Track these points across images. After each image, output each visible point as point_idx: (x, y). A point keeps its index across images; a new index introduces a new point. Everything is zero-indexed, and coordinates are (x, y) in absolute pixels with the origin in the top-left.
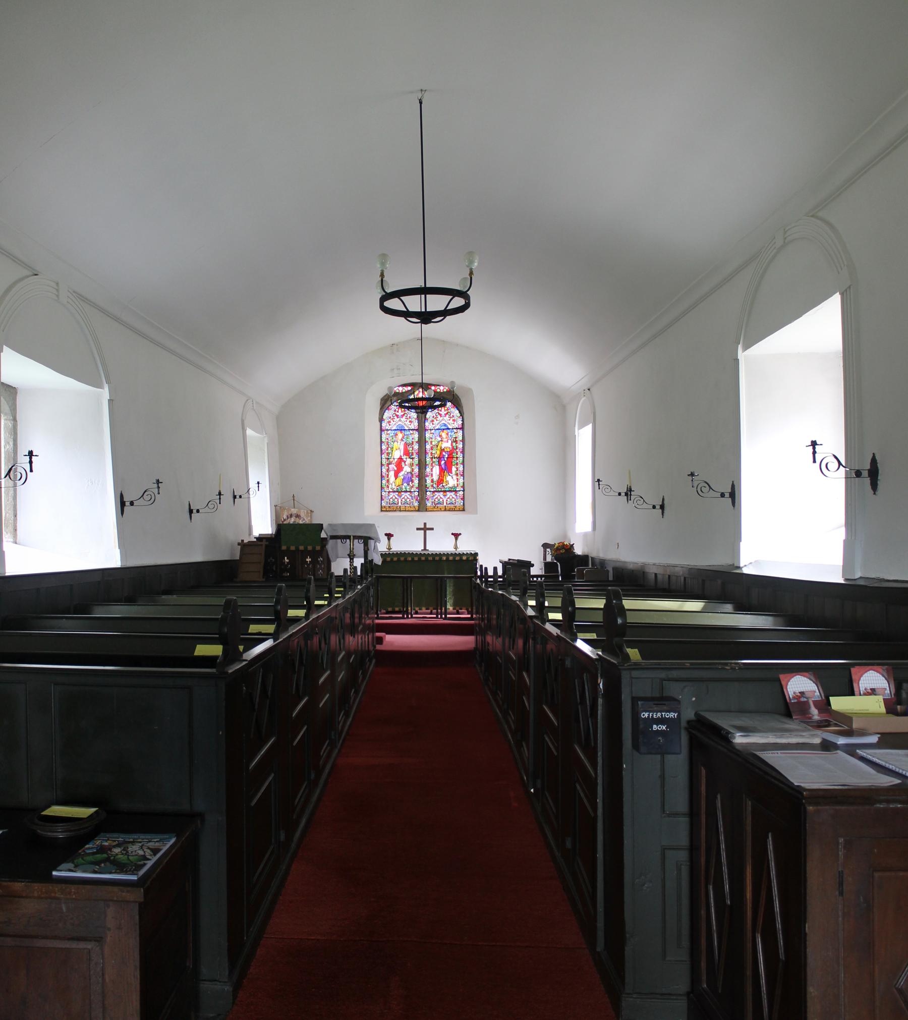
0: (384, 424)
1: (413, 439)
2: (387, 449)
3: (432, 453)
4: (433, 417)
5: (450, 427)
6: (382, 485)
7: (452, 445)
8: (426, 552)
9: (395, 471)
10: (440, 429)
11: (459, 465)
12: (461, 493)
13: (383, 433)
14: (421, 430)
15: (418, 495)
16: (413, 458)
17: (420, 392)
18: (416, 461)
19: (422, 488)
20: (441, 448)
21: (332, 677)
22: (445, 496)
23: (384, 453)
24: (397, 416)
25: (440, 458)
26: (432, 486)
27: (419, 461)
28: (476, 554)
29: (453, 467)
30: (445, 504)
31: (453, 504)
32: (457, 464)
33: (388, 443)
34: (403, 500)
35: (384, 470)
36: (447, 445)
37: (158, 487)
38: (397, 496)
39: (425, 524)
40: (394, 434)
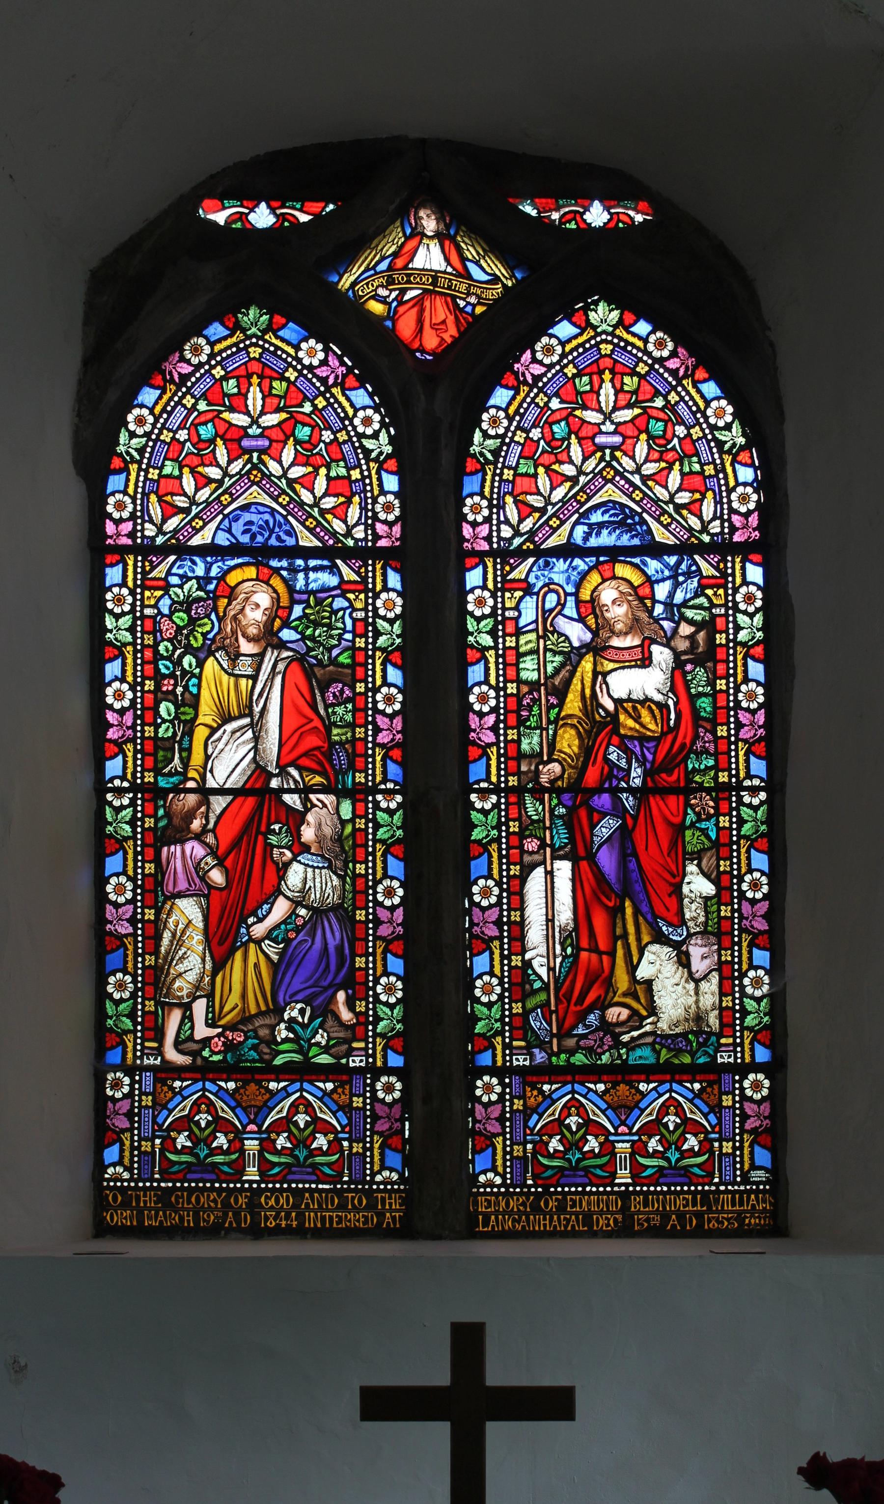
5: (661, 535)
17: (418, 234)
20: (591, 703)
29: (692, 868)
30: (624, 1176)
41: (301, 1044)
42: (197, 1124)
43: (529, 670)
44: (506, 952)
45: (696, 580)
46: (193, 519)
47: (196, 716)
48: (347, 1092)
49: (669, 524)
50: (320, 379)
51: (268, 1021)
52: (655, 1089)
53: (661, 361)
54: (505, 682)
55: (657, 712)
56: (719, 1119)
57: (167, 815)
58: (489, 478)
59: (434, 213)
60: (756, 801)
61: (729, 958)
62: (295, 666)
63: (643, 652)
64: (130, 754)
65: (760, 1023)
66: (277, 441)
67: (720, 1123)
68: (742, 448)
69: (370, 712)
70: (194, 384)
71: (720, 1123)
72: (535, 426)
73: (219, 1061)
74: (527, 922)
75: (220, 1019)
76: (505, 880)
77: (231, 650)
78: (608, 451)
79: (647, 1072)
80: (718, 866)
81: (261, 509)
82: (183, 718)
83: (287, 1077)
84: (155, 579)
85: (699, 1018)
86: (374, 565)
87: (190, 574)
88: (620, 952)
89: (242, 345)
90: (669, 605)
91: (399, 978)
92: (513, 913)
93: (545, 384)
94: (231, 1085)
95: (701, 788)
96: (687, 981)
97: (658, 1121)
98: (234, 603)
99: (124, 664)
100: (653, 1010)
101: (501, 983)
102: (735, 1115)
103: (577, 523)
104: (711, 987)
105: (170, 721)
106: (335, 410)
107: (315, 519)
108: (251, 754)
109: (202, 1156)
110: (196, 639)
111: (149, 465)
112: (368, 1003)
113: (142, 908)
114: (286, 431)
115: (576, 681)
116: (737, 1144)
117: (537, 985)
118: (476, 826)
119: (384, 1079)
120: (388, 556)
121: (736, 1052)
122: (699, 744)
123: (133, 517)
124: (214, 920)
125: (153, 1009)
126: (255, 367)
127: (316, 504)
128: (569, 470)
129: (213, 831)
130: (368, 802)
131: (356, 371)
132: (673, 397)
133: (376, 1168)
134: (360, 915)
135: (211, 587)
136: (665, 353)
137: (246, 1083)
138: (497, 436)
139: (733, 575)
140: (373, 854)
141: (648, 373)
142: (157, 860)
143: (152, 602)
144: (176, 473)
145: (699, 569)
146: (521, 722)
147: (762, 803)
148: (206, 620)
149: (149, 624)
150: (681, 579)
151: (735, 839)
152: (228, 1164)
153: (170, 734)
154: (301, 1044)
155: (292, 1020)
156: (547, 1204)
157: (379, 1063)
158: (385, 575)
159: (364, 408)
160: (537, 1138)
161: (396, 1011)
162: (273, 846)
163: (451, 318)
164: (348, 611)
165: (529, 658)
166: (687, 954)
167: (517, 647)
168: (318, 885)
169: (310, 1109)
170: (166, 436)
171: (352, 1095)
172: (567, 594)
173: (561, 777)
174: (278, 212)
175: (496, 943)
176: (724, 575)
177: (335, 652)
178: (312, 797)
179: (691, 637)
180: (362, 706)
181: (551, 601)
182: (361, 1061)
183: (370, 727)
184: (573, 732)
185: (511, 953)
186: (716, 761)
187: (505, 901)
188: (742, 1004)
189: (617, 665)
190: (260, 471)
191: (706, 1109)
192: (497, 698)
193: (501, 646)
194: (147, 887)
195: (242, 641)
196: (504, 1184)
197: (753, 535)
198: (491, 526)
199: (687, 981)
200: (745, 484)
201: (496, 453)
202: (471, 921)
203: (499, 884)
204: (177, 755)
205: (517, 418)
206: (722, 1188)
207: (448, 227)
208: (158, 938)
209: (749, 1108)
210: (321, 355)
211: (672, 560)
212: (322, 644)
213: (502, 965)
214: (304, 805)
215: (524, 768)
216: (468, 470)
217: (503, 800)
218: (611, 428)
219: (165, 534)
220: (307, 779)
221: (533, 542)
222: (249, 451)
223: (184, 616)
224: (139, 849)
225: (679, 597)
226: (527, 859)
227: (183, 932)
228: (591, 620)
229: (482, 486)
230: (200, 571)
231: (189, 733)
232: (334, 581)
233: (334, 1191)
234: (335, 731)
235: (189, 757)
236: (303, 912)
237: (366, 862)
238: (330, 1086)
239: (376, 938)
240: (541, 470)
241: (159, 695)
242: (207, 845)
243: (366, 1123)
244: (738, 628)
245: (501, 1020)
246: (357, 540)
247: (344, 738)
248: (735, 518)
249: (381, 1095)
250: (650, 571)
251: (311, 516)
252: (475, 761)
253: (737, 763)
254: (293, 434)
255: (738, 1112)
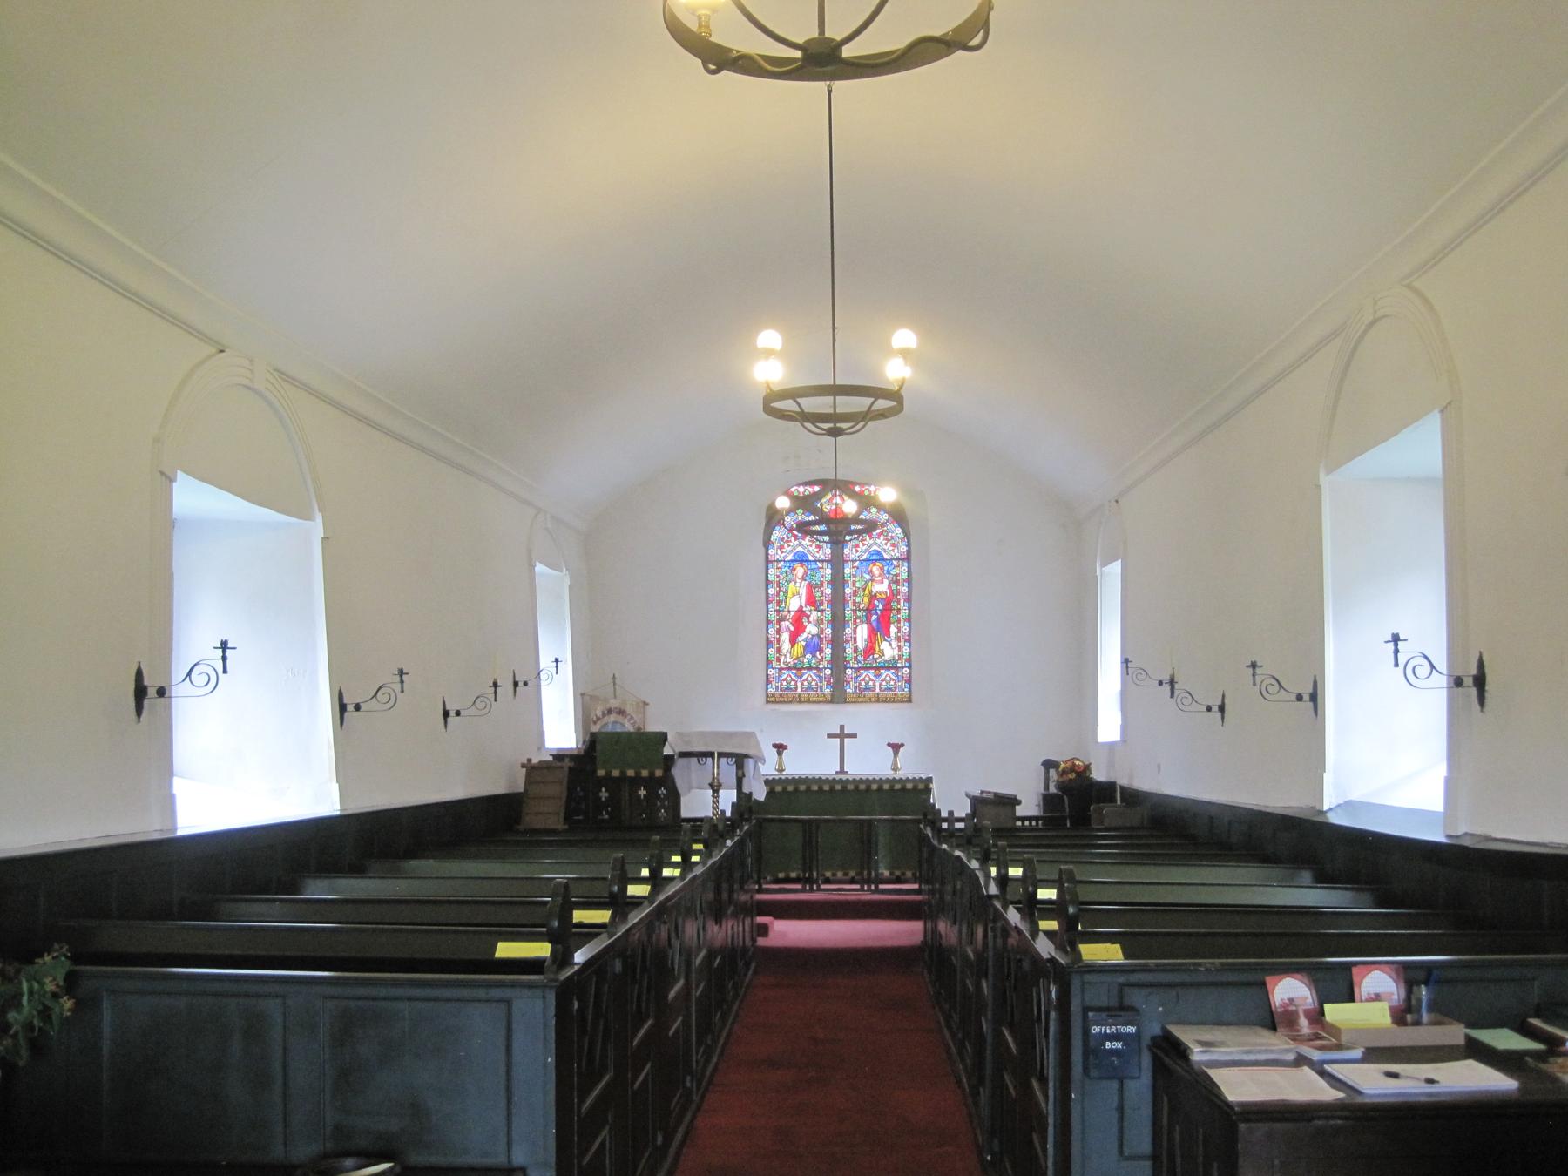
0: (771, 552)
1: (822, 577)
2: (778, 595)
3: (855, 602)
5: (886, 556)
7: (890, 587)
8: (844, 777)
9: (791, 632)
11: (902, 622)
12: (906, 671)
13: (770, 566)
14: (837, 562)
16: (822, 611)
18: (828, 613)
19: (838, 662)
21: (687, 988)
22: (878, 676)
25: (869, 610)
26: (856, 658)
27: (834, 615)
28: (929, 780)
29: (892, 625)
30: (878, 690)
31: (890, 689)
32: (899, 621)
33: (778, 583)
34: (805, 683)
35: (772, 631)
36: (881, 587)
37: (402, 682)
38: (793, 677)
39: (842, 727)
41: (809, 663)
79: (883, 668)
100: (883, 655)
154: (809, 663)
232: (815, 566)
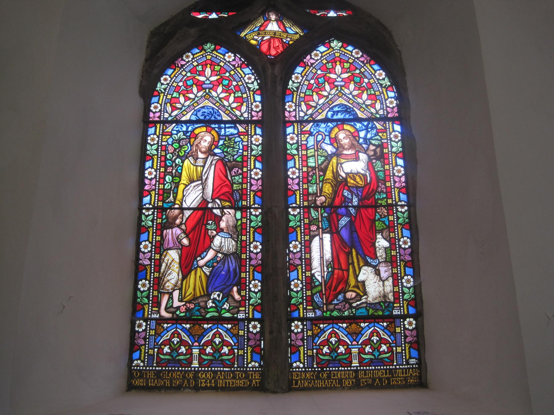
1: (245, 148)
2: (162, 180)
3: (306, 194)
4: (310, 87)
5: (360, 115)
6: (135, 297)
7: (370, 165)
9: (182, 248)
10: (331, 121)
12: (410, 323)
15: (262, 332)
17: (269, 20)
20: (336, 175)
22: (355, 335)
23: (149, 192)
24: (200, 85)
26: (310, 300)
29: (379, 236)
30: (355, 363)
31: (382, 362)
32: (391, 227)
38: (185, 338)
40: (185, 133)
41: (218, 309)
42: (173, 342)
43: (312, 162)
44: (304, 270)
45: (375, 130)
46: (183, 111)
47: (180, 180)
48: (237, 328)
49: (364, 111)
50: (232, 65)
51: (204, 299)
52: (367, 326)
53: (358, 58)
54: (302, 167)
55: (362, 177)
56: (395, 338)
57: (167, 218)
58: (295, 96)
59: (274, 13)
60: (403, 210)
61: (396, 272)
62: (219, 162)
63: (356, 156)
64: (153, 195)
65: (410, 297)
66: (216, 85)
67: (396, 340)
68: (389, 86)
69: (249, 179)
70: (186, 68)
71: (396, 340)
72: (312, 79)
73: (184, 316)
74: (312, 258)
75: (184, 298)
76: (303, 242)
77: (195, 157)
78: (339, 87)
79: (364, 319)
80: (390, 235)
81: (209, 107)
82: (175, 181)
83: (212, 322)
84: (167, 132)
85: (385, 296)
86: (251, 126)
87: (180, 130)
88: (351, 270)
89: (204, 55)
90: (365, 139)
91: (259, 281)
92: (306, 255)
93: (315, 66)
94: (188, 326)
95: (381, 205)
96: (379, 281)
97: (369, 339)
98: (197, 140)
99: (153, 162)
100: (365, 293)
101: (302, 283)
102: (402, 336)
103: (329, 111)
104: (389, 283)
105: (169, 183)
106: (238, 75)
107: (229, 111)
108: (201, 195)
109: (174, 356)
110: (181, 153)
111: (168, 94)
112: (246, 292)
113: (155, 254)
114: (219, 82)
115: (330, 168)
116: (403, 348)
117: (317, 283)
118: (291, 221)
119: (253, 323)
120: (257, 123)
121: (401, 310)
122: (379, 189)
123: (160, 111)
124: (183, 259)
125: (157, 294)
126: (209, 62)
127: (230, 106)
128: (325, 93)
129: (185, 224)
130: (247, 212)
131: (246, 63)
132: (363, 70)
133: (249, 361)
134: (244, 256)
135: (188, 134)
136: (359, 56)
137: (194, 325)
138: (298, 83)
139: (389, 128)
140: (249, 232)
141: (353, 62)
142: (161, 235)
143: (166, 140)
144: (178, 96)
145: (376, 127)
146: (309, 182)
147: (406, 211)
148: (186, 146)
149: (164, 148)
150: (369, 130)
151: (396, 224)
152: (185, 360)
153: (169, 187)
154: (218, 309)
155: (214, 299)
156: (322, 375)
157: (251, 316)
158: (255, 129)
159: (248, 74)
160: (318, 347)
161: (258, 295)
162: (208, 230)
163: (281, 45)
164: (241, 142)
165: (311, 158)
166: (379, 270)
167: (307, 154)
168: (226, 244)
169: (221, 336)
170: (175, 84)
171: (239, 330)
172: (325, 135)
173: (325, 202)
174: (219, 15)
175: (300, 267)
176: (386, 128)
177: (235, 157)
178: (225, 210)
179: (374, 151)
180: (246, 176)
181: (320, 138)
182: (243, 315)
183: (249, 184)
184: (329, 185)
185: (306, 271)
186: (387, 195)
187: (303, 250)
188: (402, 290)
189: (346, 161)
190: (209, 95)
191: (389, 334)
192: (299, 173)
193: (300, 154)
194: (157, 246)
195: (199, 153)
196: (304, 367)
197: (396, 115)
198: (296, 112)
199: (379, 281)
200: (391, 98)
201: (297, 88)
202: (289, 258)
203: (301, 243)
204: (172, 195)
205: (305, 77)
206: (398, 367)
207: (279, 17)
208: (160, 266)
209: (407, 333)
210: (233, 58)
211: (366, 123)
212: (230, 154)
213: (302, 276)
214: (222, 213)
215: (310, 199)
216: (287, 94)
217: (302, 211)
218: (341, 80)
219: (172, 116)
220: (223, 204)
221: (312, 117)
222: (205, 89)
223: (177, 145)
224: (154, 231)
225: (369, 136)
226: (312, 233)
227: (171, 264)
228: (335, 145)
229: (293, 99)
230: (184, 129)
231: (177, 187)
232: (236, 132)
233: (231, 371)
234: (235, 186)
235: (176, 196)
236: (220, 255)
237: (246, 235)
238: (230, 326)
239: (250, 265)
240: (314, 93)
241: (166, 173)
242: (182, 229)
243: (244, 342)
244: (392, 147)
245: (302, 298)
246: (245, 118)
247: (238, 188)
248: (388, 109)
249: (251, 330)
250: (358, 127)
251: (227, 110)
252: (290, 196)
253: (395, 196)
254: (222, 83)
255: (403, 334)
